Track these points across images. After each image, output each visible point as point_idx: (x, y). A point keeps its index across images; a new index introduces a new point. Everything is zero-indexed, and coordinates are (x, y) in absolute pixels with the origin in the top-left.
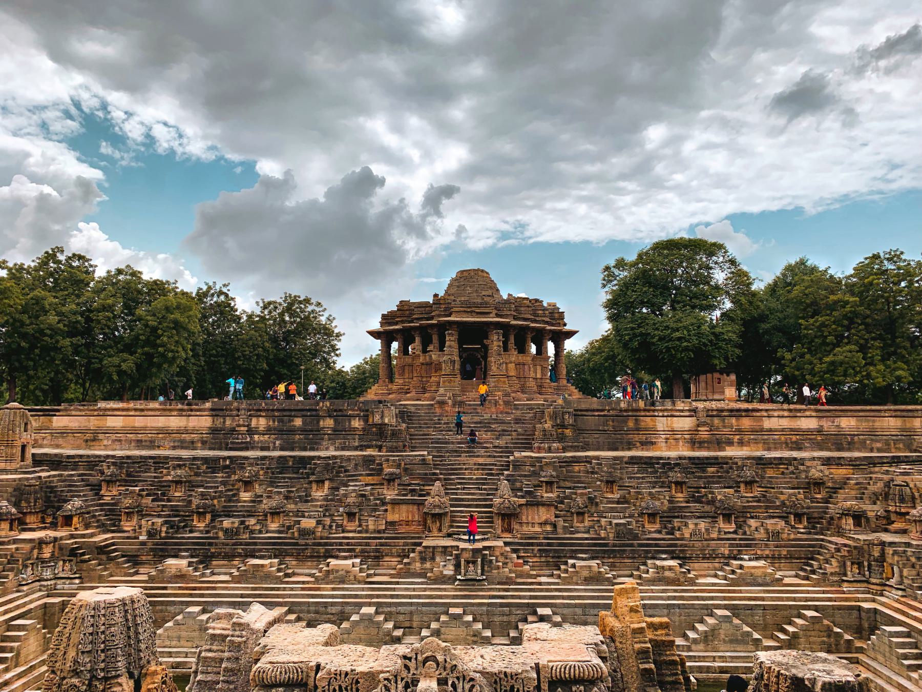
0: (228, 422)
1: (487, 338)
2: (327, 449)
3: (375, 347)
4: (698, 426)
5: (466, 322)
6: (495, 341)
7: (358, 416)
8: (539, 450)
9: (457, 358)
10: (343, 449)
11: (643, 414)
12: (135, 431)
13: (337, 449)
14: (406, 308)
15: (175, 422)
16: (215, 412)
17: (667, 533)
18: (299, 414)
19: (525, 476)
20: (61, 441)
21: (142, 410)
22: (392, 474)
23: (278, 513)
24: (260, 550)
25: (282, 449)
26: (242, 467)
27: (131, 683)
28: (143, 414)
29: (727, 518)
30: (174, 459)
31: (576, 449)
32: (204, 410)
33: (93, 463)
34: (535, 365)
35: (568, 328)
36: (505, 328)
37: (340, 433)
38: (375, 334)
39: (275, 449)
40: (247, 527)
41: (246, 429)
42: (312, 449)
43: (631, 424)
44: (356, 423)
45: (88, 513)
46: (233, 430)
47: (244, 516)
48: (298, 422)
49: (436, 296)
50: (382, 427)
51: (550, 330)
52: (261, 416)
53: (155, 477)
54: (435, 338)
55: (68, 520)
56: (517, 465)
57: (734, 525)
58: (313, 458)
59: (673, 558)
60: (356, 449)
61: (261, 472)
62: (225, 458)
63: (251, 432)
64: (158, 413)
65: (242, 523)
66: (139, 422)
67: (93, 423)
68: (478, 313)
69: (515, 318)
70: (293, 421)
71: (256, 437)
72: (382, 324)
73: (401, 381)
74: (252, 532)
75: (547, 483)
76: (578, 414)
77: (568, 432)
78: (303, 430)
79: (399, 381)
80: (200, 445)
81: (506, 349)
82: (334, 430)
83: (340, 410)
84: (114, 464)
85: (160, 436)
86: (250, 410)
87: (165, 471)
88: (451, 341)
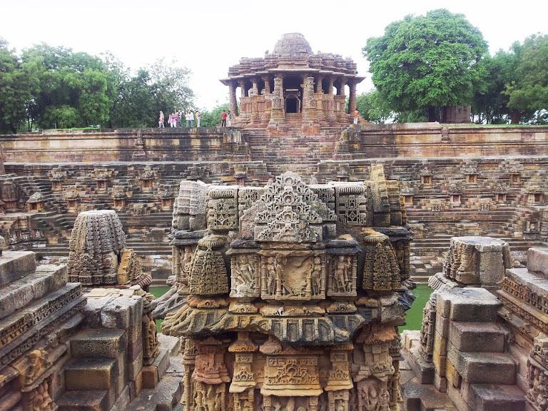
0: (130, 143)
1: (302, 82)
2: (197, 159)
4: (442, 140)
6: (308, 85)
7: (216, 138)
8: (338, 157)
9: (282, 98)
10: (207, 159)
11: (406, 133)
12: (68, 149)
13: (203, 160)
14: (246, 62)
16: (121, 136)
17: (417, 208)
18: (177, 136)
19: (328, 174)
20: (20, 157)
21: (72, 136)
22: (241, 175)
23: (168, 200)
24: (159, 222)
25: (167, 160)
26: (142, 171)
27: (116, 256)
28: (73, 138)
29: (456, 197)
30: (97, 167)
31: (360, 157)
32: (113, 135)
33: (44, 170)
34: (336, 102)
35: (357, 76)
36: (315, 76)
37: (205, 150)
38: (226, 82)
39: (163, 160)
40: (149, 209)
41: (142, 147)
42: (187, 160)
43: (398, 140)
44: (215, 143)
45: (46, 201)
46: (134, 147)
47: (146, 202)
48: (176, 142)
49: (267, 52)
50: (232, 144)
51: (347, 77)
52: (150, 138)
53: (85, 179)
54: (267, 84)
55: (34, 205)
56: (322, 167)
57: (460, 202)
58: (188, 165)
59: (419, 222)
60: (216, 159)
61: (155, 175)
62: (130, 166)
63: (145, 149)
64: (83, 137)
65: (145, 206)
66: (71, 144)
67: (39, 145)
68: (296, 65)
70: (171, 141)
71: (149, 152)
72: (229, 74)
73: (244, 115)
74: (153, 211)
75: (341, 178)
76: (362, 134)
77: (356, 146)
79: (242, 114)
80: (113, 158)
81: (315, 91)
82: (201, 147)
83: (204, 134)
84: (58, 171)
85: (86, 153)
86: (143, 135)
87: (92, 175)
88: (278, 83)
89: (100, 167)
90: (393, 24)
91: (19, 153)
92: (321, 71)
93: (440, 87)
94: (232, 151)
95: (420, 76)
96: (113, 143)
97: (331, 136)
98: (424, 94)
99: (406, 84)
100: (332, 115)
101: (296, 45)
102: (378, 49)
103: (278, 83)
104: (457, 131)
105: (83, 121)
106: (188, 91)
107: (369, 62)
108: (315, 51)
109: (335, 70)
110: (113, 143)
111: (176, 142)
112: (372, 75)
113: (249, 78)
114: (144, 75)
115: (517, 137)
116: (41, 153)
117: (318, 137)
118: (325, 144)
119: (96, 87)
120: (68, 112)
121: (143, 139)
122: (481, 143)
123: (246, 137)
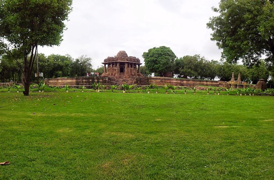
3: (103, 65)
5: (121, 62)
6: (126, 66)
9: (119, 69)
15: (69, 81)
16: (76, 79)
34: (134, 70)
35: (141, 63)
37: (98, 82)
44: (101, 80)
48: (91, 80)
63: (83, 82)
67: (56, 81)
69: (130, 61)
78: (92, 82)
81: (128, 67)
88: (118, 65)
89: (72, 87)
90: (150, 49)
91: (51, 83)
92: (130, 62)
93: (162, 67)
94: (105, 83)
95: (157, 64)
96: (74, 81)
97: (132, 79)
98: (158, 69)
99: (153, 66)
100: (133, 74)
101: (123, 54)
102: (146, 55)
103: (118, 65)
104: (164, 79)
105: (64, 75)
106: (90, 65)
107: (144, 59)
108: (129, 56)
109: (134, 62)
110: (74, 81)
111: (91, 80)
112: (145, 62)
113: (110, 62)
114: (78, 60)
115: (179, 82)
116: (56, 84)
117: (129, 79)
118: (130, 81)
119: (67, 65)
120: (60, 72)
121: (82, 80)
122: (170, 82)
123: (109, 79)
